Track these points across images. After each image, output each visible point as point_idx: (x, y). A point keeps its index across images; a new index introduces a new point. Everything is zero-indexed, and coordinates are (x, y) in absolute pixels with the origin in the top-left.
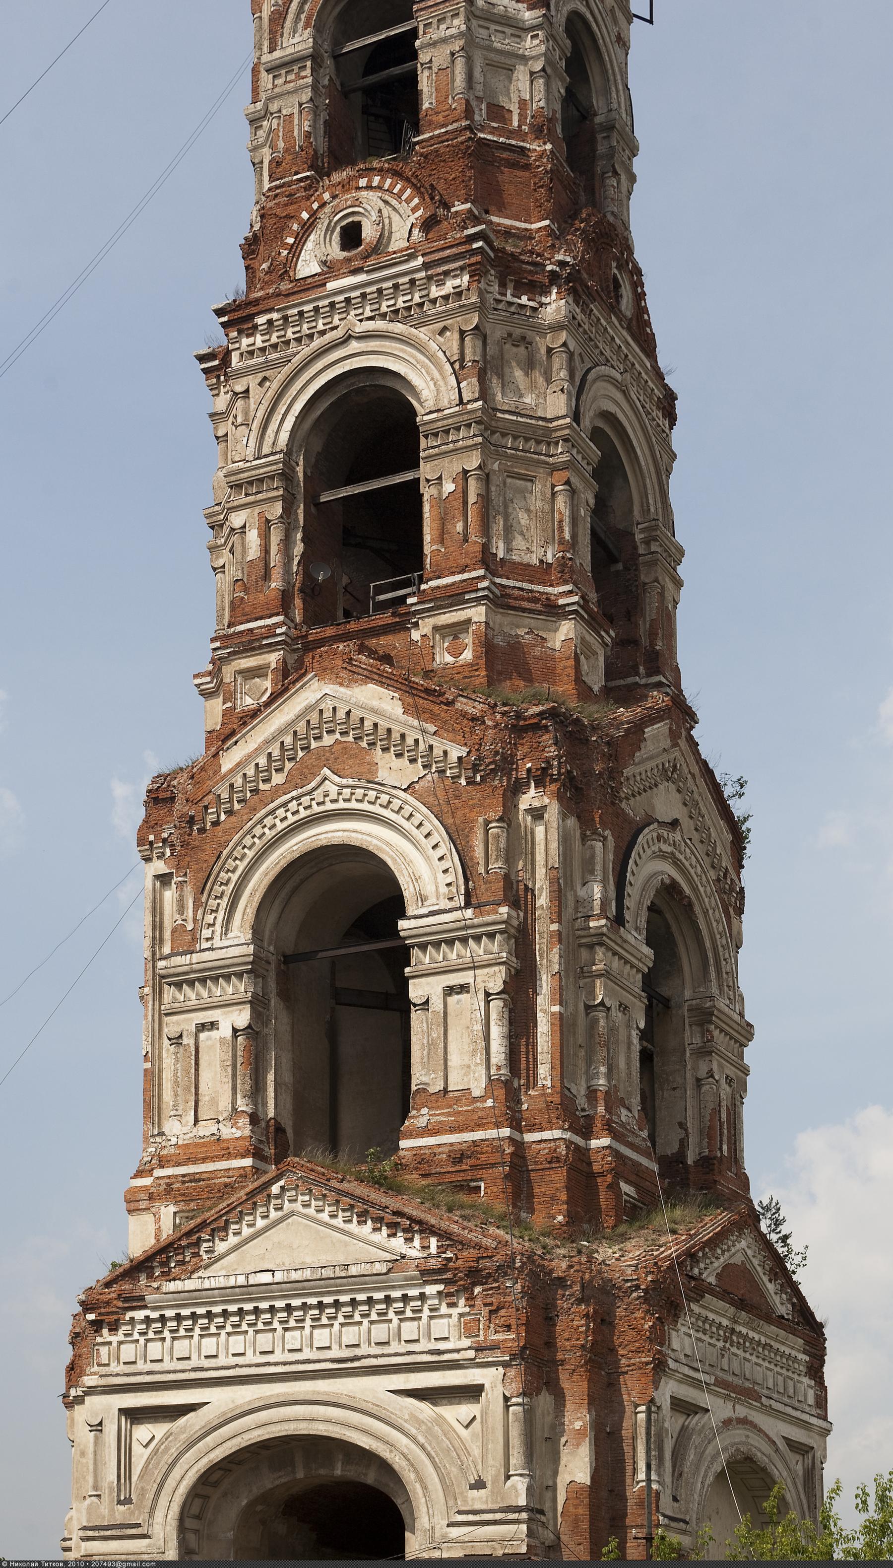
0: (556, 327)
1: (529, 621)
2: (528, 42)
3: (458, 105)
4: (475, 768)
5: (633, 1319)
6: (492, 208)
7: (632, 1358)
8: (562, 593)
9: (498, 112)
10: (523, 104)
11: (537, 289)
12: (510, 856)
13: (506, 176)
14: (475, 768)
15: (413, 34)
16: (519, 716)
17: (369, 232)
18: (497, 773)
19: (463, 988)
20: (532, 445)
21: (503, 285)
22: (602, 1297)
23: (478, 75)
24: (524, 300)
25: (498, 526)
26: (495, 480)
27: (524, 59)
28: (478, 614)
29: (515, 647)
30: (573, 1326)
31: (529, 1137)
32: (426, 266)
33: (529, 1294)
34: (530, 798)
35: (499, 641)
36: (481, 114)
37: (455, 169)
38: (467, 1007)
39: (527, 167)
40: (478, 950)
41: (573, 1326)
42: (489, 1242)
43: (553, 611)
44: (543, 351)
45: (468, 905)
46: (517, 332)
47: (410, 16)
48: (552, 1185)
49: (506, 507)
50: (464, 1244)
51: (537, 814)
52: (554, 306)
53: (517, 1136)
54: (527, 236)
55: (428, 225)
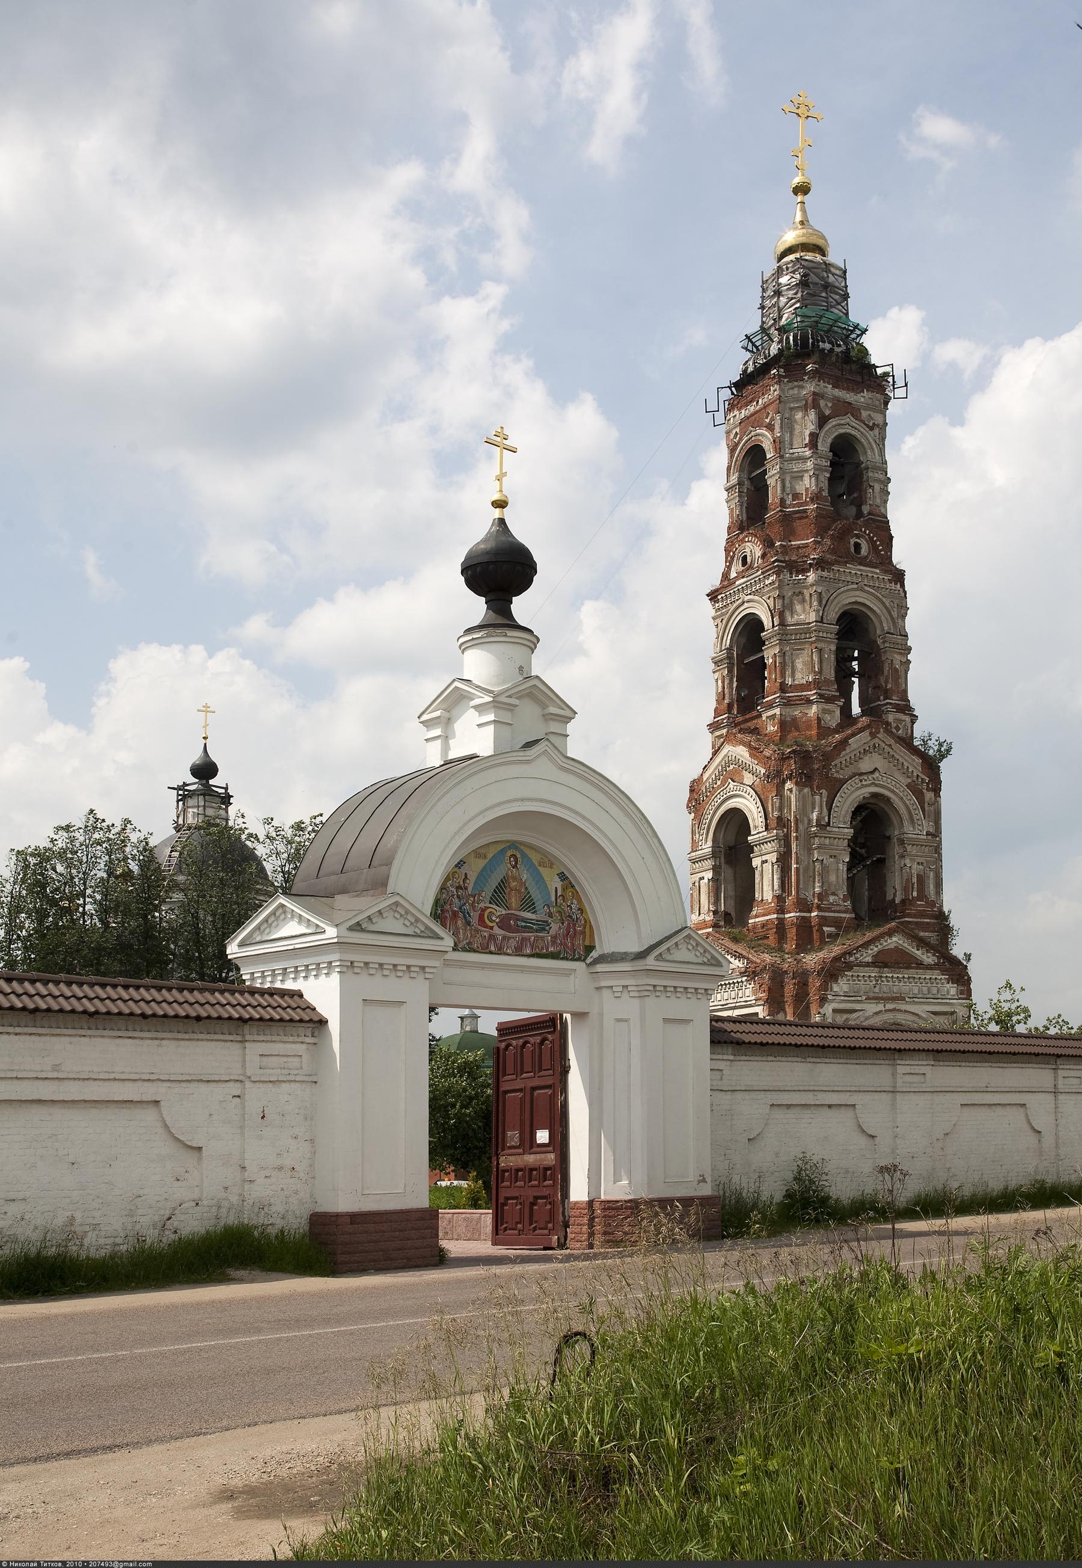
0: (812, 585)
1: (800, 708)
2: (809, 463)
3: (777, 501)
4: (768, 777)
5: (815, 983)
6: (791, 538)
7: (813, 997)
8: (812, 694)
9: (796, 496)
10: (807, 489)
11: (804, 571)
12: (781, 809)
13: (797, 524)
14: (768, 777)
15: (765, 472)
16: (783, 754)
17: (749, 560)
18: (776, 778)
19: (766, 861)
20: (803, 636)
21: (791, 574)
22: (802, 978)
23: (788, 484)
24: (800, 577)
25: (788, 672)
26: (787, 654)
27: (807, 471)
28: (777, 711)
29: (794, 719)
30: (790, 989)
31: (787, 916)
32: (763, 573)
33: (771, 979)
34: (788, 785)
35: (788, 719)
36: (789, 500)
37: (777, 528)
38: (767, 867)
39: (807, 517)
40: (768, 847)
41: (790, 989)
42: (758, 961)
43: (809, 702)
44: (807, 598)
45: (767, 829)
46: (797, 591)
47: (764, 465)
48: (792, 934)
49: (793, 663)
50: (752, 962)
51: (791, 790)
52: (812, 576)
53: (781, 916)
54: (806, 546)
55: (763, 556)
